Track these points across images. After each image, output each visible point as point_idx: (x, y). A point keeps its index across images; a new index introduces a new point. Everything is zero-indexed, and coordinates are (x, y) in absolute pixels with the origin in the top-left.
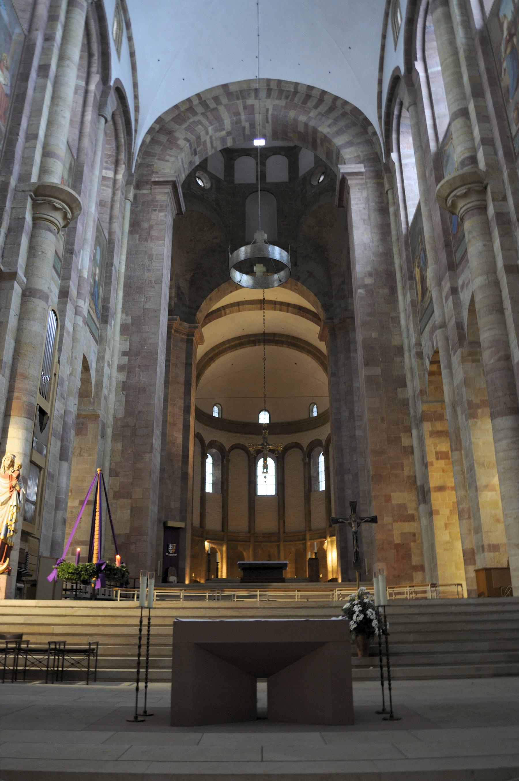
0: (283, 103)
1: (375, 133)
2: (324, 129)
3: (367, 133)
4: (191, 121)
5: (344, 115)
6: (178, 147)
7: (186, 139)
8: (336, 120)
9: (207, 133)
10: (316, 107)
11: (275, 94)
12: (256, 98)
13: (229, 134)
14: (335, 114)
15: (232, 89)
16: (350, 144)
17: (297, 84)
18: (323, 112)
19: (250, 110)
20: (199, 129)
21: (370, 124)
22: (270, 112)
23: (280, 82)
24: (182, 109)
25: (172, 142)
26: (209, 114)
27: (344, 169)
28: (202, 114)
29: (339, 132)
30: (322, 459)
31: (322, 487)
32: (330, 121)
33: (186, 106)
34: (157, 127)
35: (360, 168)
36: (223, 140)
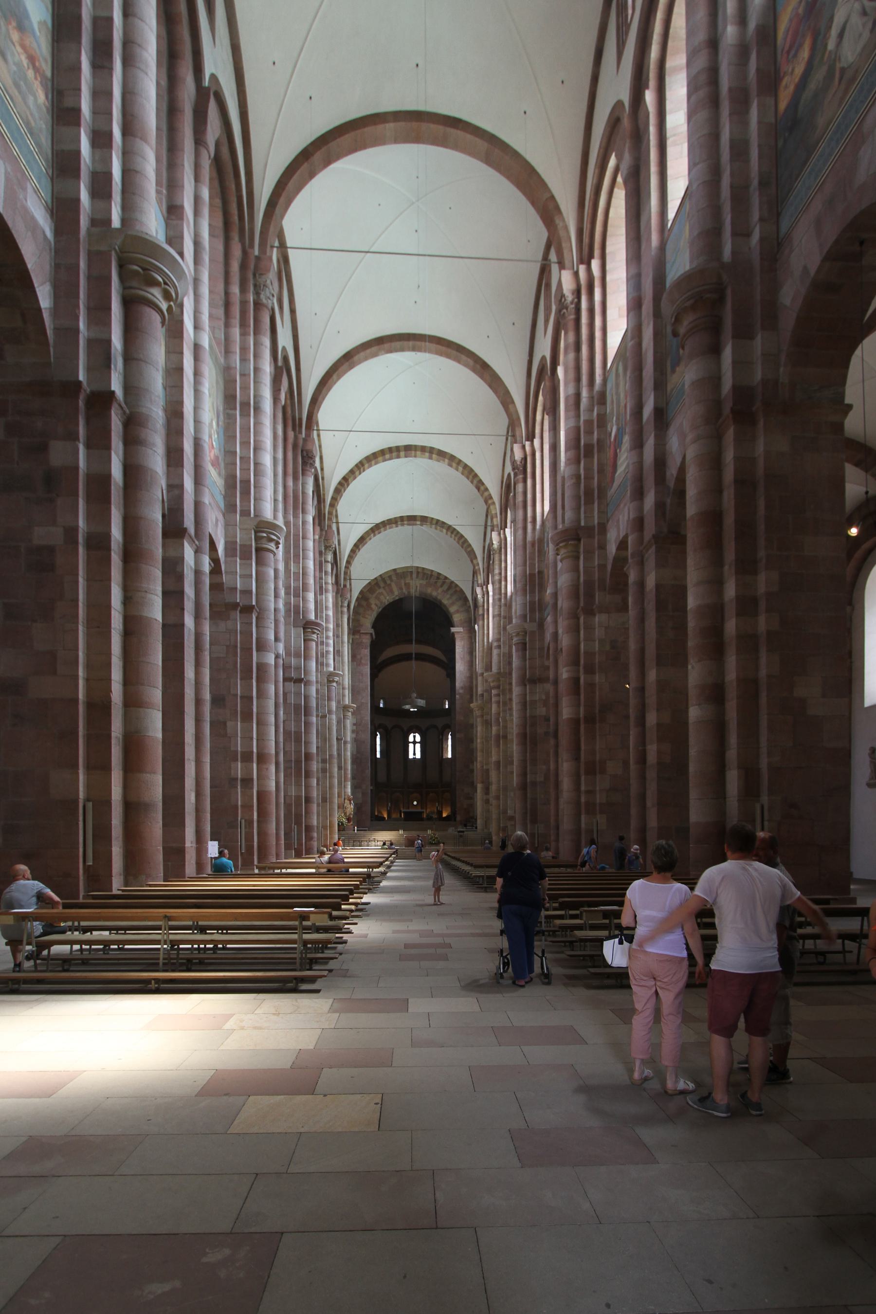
0: (424, 582)
1: (470, 607)
2: (445, 602)
3: (466, 604)
4: (378, 592)
5: (456, 592)
6: (371, 609)
7: (377, 605)
8: (452, 595)
9: (386, 598)
10: (441, 586)
11: (421, 575)
12: (412, 579)
13: (396, 596)
14: (450, 592)
15: (398, 571)
16: (457, 611)
17: (432, 571)
18: (445, 590)
19: (407, 585)
20: (382, 597)
21: (468, 601)
22: (418, 588)
23: (423, 568)
24: (373, 584)
25: (369, 606)
26: (387, 587)
27: (453, 630)
28: (384, 587)
29: (453, 604)
30: (450, 737)
31: (450, 756)
32: (448, 596)
33: (375, 581)
34: (360, 596)
35: (460, 629)
36: (393, 598)
